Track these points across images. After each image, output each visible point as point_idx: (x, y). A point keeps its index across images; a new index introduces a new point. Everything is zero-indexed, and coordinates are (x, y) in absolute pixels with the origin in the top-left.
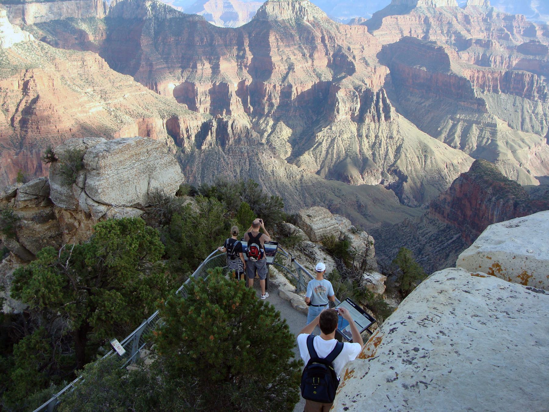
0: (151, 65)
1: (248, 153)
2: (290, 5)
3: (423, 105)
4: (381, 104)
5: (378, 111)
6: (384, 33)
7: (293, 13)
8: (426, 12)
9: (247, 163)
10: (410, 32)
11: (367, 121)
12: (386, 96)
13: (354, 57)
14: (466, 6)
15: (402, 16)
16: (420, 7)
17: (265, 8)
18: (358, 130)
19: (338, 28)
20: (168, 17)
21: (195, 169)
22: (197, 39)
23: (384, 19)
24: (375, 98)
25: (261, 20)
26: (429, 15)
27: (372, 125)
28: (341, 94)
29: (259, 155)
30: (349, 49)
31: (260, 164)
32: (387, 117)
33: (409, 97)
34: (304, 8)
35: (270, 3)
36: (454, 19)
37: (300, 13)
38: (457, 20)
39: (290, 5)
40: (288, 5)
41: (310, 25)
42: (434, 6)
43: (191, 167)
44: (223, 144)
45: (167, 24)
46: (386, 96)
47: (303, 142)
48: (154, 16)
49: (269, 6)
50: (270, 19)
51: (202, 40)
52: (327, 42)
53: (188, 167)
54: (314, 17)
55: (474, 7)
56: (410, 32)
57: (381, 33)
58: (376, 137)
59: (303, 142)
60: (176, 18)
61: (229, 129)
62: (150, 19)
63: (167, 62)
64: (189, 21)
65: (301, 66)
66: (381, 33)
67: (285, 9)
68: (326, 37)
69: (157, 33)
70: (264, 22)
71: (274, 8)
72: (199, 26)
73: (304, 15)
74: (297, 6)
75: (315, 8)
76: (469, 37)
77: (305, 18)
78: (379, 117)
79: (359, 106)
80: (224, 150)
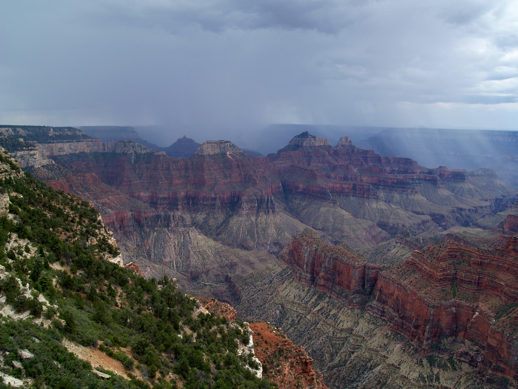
0: (130, 181)
1: (183, 232)
4: (269, 203)
5: (268, 208)
8: (309, 149)
9: (182, 238)
11: (261, 215)
12: (273, 198)
13: (257, 177)
16: (306, 146)
18: (256, 220)
19: (249, 159)
20: (143, 152)
21: (150, 241)
22: (159, 166)
24: (266, 199)
26: (311, 151)
27: (265, 216)
28: (244, 198)
29: (190, 232)
30: (255, 172)
31: (190, 238)
32: (274, 212)
33: (293, 200)
36: (327, 153)
43: (148, 240)
44: (168, 226)
45: (142, 156)
46: (273, 198)
47: (222, 228)
48: (135, 151)
51: (163, 166)
53: (146, 241)
58: (266, 224)
59: (222, 228)
60: (148, 153)
61: (172, 218)
62: (132, 153)
63: (140, 180)
64: (156, 155)
69: (135, 162)
70: (201, 155)
72: (161, 158)
74: (222, 146)
76: (336, 163)
77: (228, 153)
78: (268, 212)
79: (256, 205)
80: (168, 230)
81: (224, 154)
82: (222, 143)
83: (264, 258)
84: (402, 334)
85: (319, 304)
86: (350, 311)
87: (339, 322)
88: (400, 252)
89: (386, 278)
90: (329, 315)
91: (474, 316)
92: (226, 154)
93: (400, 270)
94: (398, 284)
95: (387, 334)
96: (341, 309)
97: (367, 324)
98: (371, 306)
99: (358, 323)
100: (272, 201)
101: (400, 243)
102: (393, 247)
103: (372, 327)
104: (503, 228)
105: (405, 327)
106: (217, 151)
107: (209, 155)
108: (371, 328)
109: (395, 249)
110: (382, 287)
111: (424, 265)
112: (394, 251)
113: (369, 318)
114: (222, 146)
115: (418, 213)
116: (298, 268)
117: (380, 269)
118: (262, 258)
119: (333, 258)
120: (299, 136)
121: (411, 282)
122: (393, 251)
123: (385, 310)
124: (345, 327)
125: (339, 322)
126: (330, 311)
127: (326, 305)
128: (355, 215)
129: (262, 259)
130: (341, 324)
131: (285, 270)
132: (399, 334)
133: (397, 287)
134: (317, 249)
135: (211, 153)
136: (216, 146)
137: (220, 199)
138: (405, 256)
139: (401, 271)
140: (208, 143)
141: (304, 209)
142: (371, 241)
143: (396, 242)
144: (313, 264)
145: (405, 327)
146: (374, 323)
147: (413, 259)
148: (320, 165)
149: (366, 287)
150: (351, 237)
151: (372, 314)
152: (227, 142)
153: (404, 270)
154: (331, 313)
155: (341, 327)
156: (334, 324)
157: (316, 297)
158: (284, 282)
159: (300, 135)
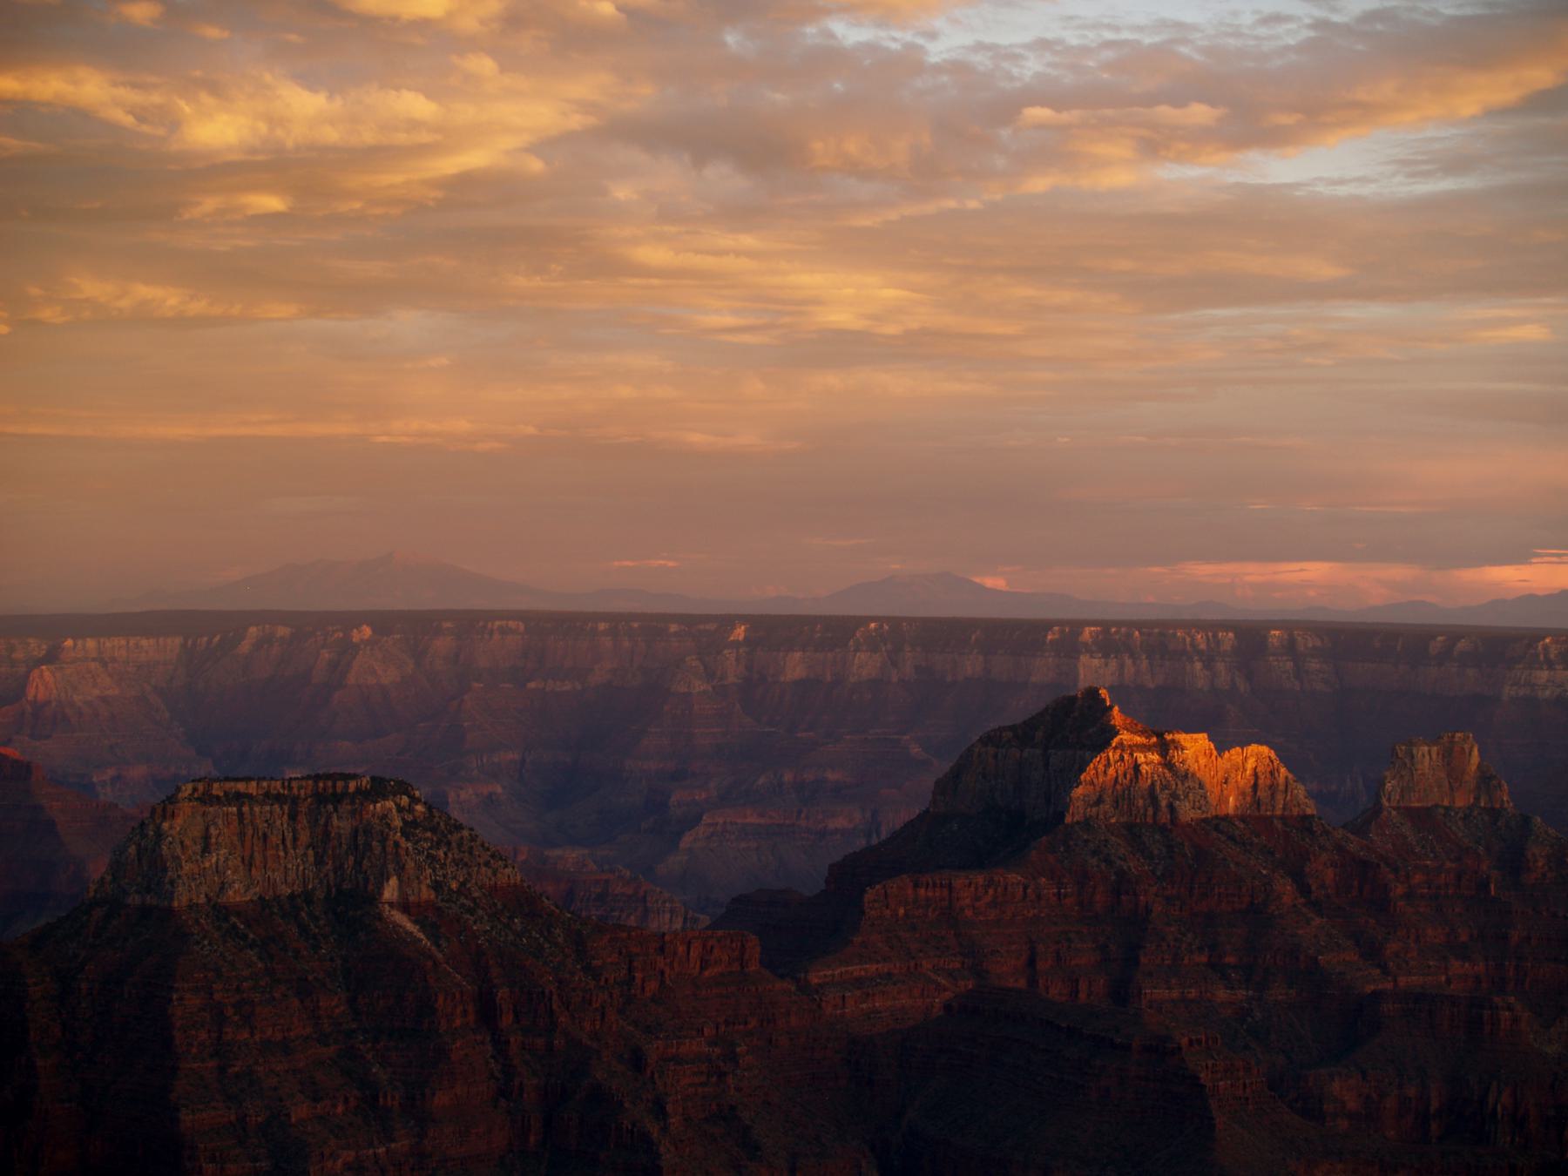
2: (303, 821)
6: (872, 968)
7: (319, 861)
10: (1032, 962)
14: (1377, 810)
15: (980, 879)
16: (1087, 824)
17: (159, 835)
23: (870, 895)
25: (134, 900)
30: (637, 1061)
34: (384, 839)
35: (185, 808)
36: (1285, 888)
37: (358, 863)
38: (1304, 890)
39: (303, 821)
40: (293, 817)
41: (410, 926)
42: (1164, 817)
49: (179, 821)
50: (181, 899)
52: (507, 1020)
54: (437, 886)
55: (1421, 817)
56: (1032, 962)
57: (855, 970)
65: (349, 1155)
66: (855, 970)
67: (275, 839)
68: (502, 993)
71: (206, 837)
73: (383, 877)
74: (342, 825)
75: (455, 838)
77: (390, 891)
81: (350, 905)
82: (337, 799)
92: (373, 899)
106: (290, 871)
107: (221, 912)
114: (342, 825)
120: (1024, 733)
135: (238, 893)
136: (282, 823)
140: (207, 799)
148: (1222, 994)
152: (379, 788)
159: (1030, 725)
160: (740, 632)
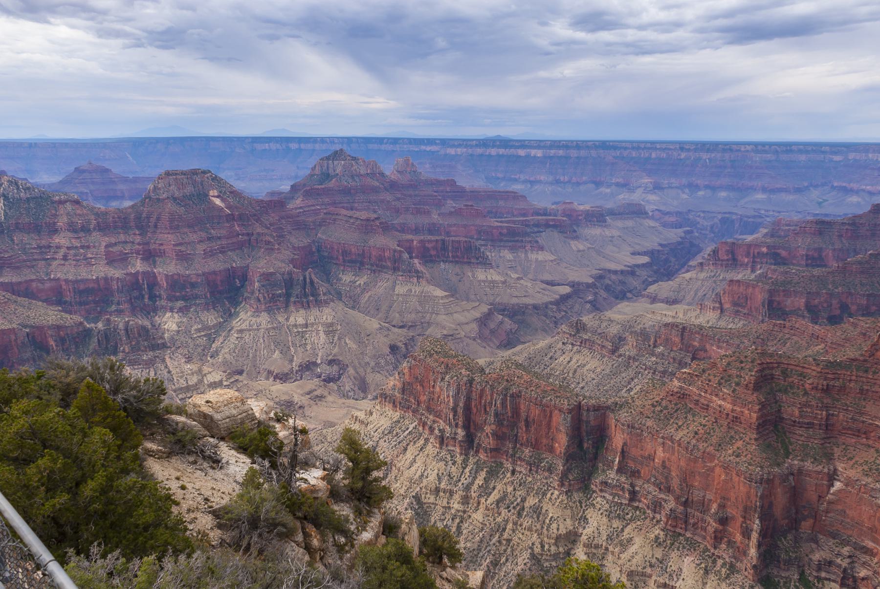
3: (358, 283)
29: (168, 360)
31: (169, 372)
74: (198, 178)
82: (197, 174)
83: (318, 392)
84: (688, 535)
85: (494, 488)
86: (565, 497)
87: (547, 521)
88: (574, 360)
89: (633, 427)
90: (523, 509)
91: (832, 490)
92: (208, 195)
93: (658, 408)
94: (663, 438)
95: (657, 538)
96: (544, 494)
97: (605, 519)
98: (606, 483)
99: (586, 519)
100: (312, 282)
101: (572, 344)
102: (559, 353)
103: (616, 524)
104: (721, 303)
105: (692, 521)
108: (615, 526)
109: (564, 356)
110: (625, 444)
111: (714, 398)
112: (562, 359)
113: (607, 506)
115: (552, 284)
116: (431, 417)
117: (608, 408)
118: (316, 393)
119: (512, 396)
121: (696, 433)
122: (562, 359)
123: (637, 488)
124: (563, 531)
125: (547, 521)
126: (524, 500)
127: (510, 489)
128: (452, 292)
129: (317, 396)
130: (554, 526)
131: (399, 422)
132: (680, 534)
133: (663, 443)
134: (473, 379)
137: (208, 285)
138: (587, 367)
139: (661, 411)
141: (364, 291)
142: (491, 340)
143: (563, 343)
144: (468, 409)
145: (692, 521)
146: (619, 517)
147: (681, 388)
149: (585, 445)
150: (459, 336)
151: (611, 498)
152: (204, 172)
153: (666, 408)
154: (527, 505)
155: (555, 531)
156: (539, 527)
157: (483, 474)
158: (406, 449)
160: (250, 140)
